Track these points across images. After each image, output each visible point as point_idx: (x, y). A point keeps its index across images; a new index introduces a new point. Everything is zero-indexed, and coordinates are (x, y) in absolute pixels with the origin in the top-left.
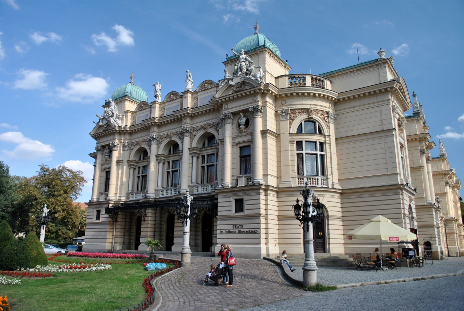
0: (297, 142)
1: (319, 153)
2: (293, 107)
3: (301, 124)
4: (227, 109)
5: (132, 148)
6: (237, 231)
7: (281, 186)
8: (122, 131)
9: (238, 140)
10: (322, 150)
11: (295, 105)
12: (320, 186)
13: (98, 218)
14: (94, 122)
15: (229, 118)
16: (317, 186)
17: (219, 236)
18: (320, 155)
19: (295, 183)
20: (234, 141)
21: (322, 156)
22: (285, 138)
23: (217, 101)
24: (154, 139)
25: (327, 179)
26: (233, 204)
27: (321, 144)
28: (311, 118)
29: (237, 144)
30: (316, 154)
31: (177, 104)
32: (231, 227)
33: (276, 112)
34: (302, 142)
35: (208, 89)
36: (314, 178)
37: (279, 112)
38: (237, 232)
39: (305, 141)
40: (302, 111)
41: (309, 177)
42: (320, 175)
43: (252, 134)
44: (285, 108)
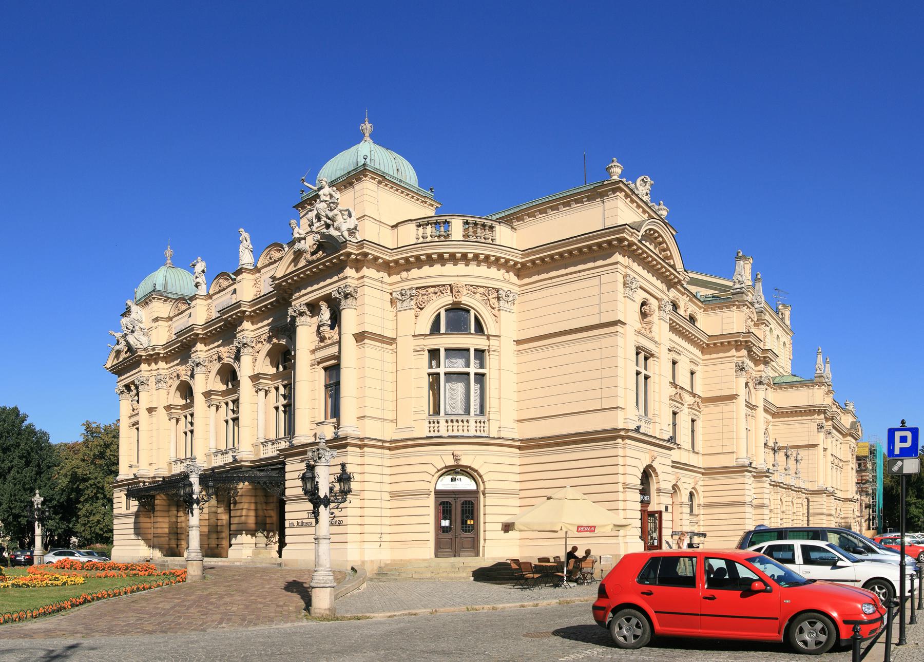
0: (429, 351)
1: (473, 370)
5: (169, 384)
11: (426, 278)
12: (472, 433)
13: (128, 508)
16: (466, 434)
18: (476, 374)
19: (422, 430)
20: (313, 357)
21: (480, 377)
22: (406, 345)
27: (480, 353)
28: (460, 303)
30: (468, 374)
34: (438, 350)
36: (460, 418)
37: (394, 294)
39: (446, 350)
40: (439, 289)
41: (449, 418)
44: (406, 285)
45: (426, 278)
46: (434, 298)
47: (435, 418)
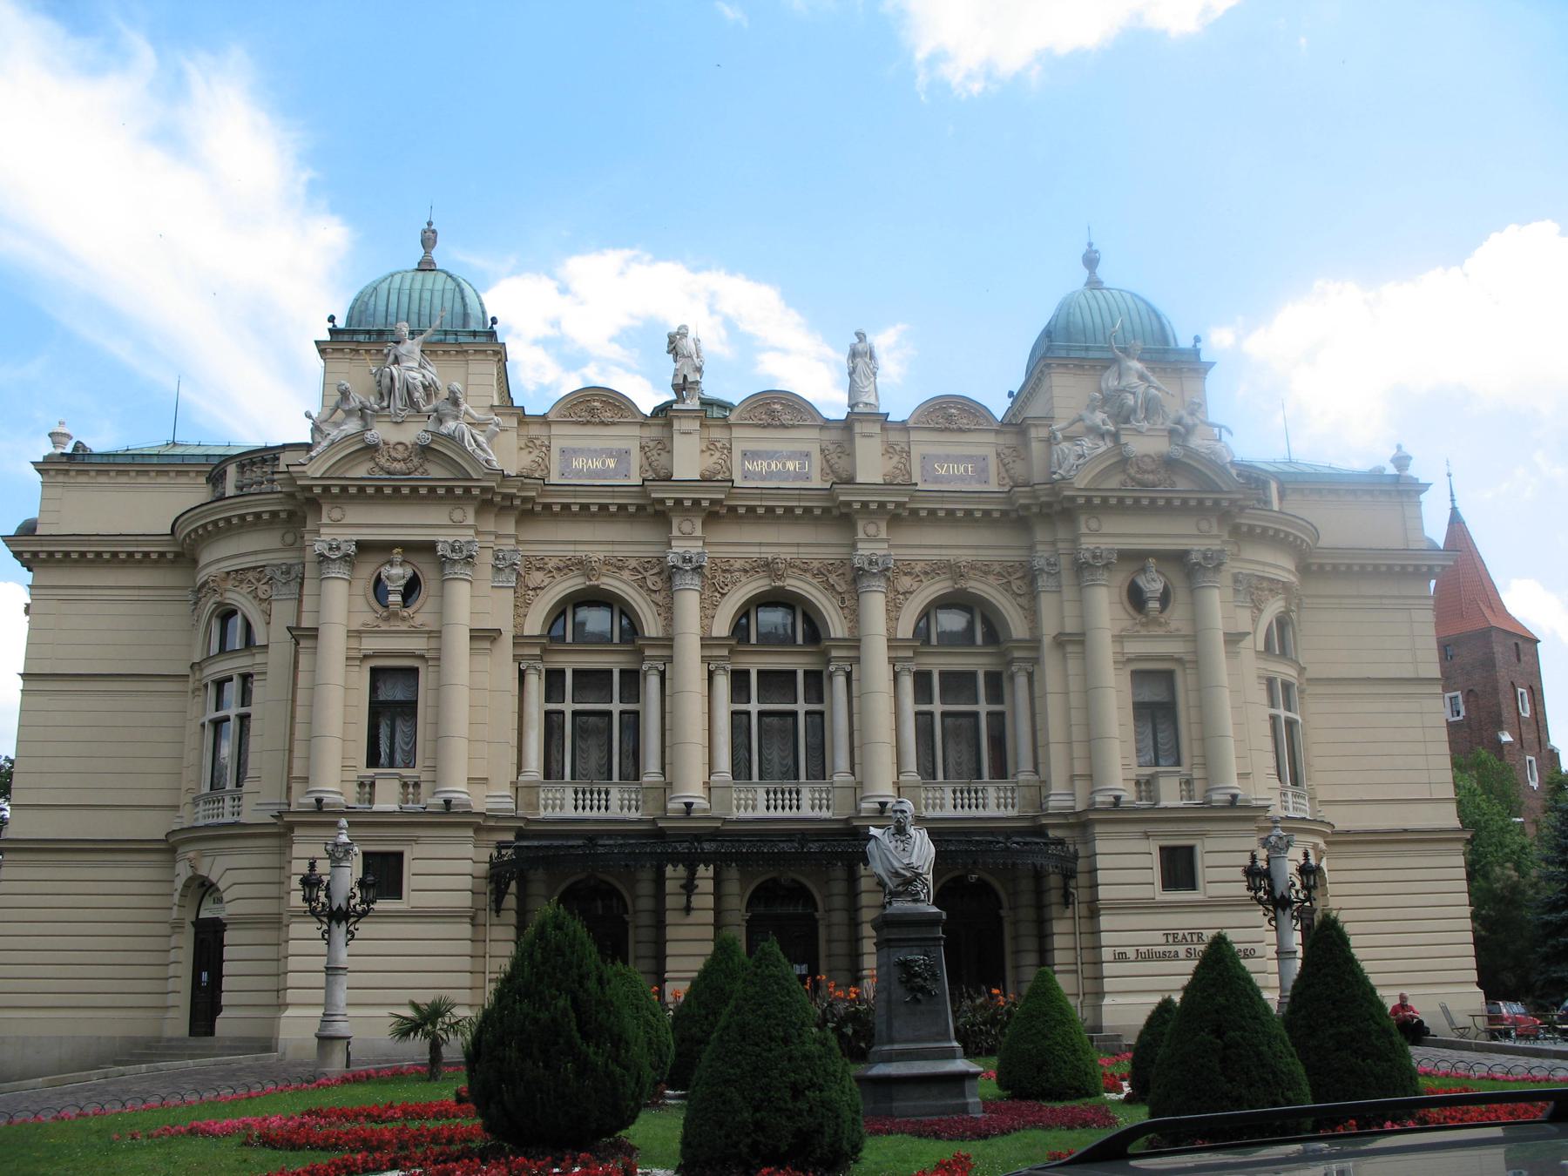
2: (1258, 570)
4: (1095, 533)
6: (1182, 950)
8: (505, 496)
9: (1134, 648)
14: (308, 415)
15: (1107, 566)
17: (1107, 969)
23: (1073, 499)
24: (698, 569)
26: (1155, 861)
29: (1129, 660)
31: (805, 447)
32: (1159, 937)
35: (960, 430)
38: (1182, 954)
40: (1277, 587)
43: (1195, 637)
45: (1264, 564)
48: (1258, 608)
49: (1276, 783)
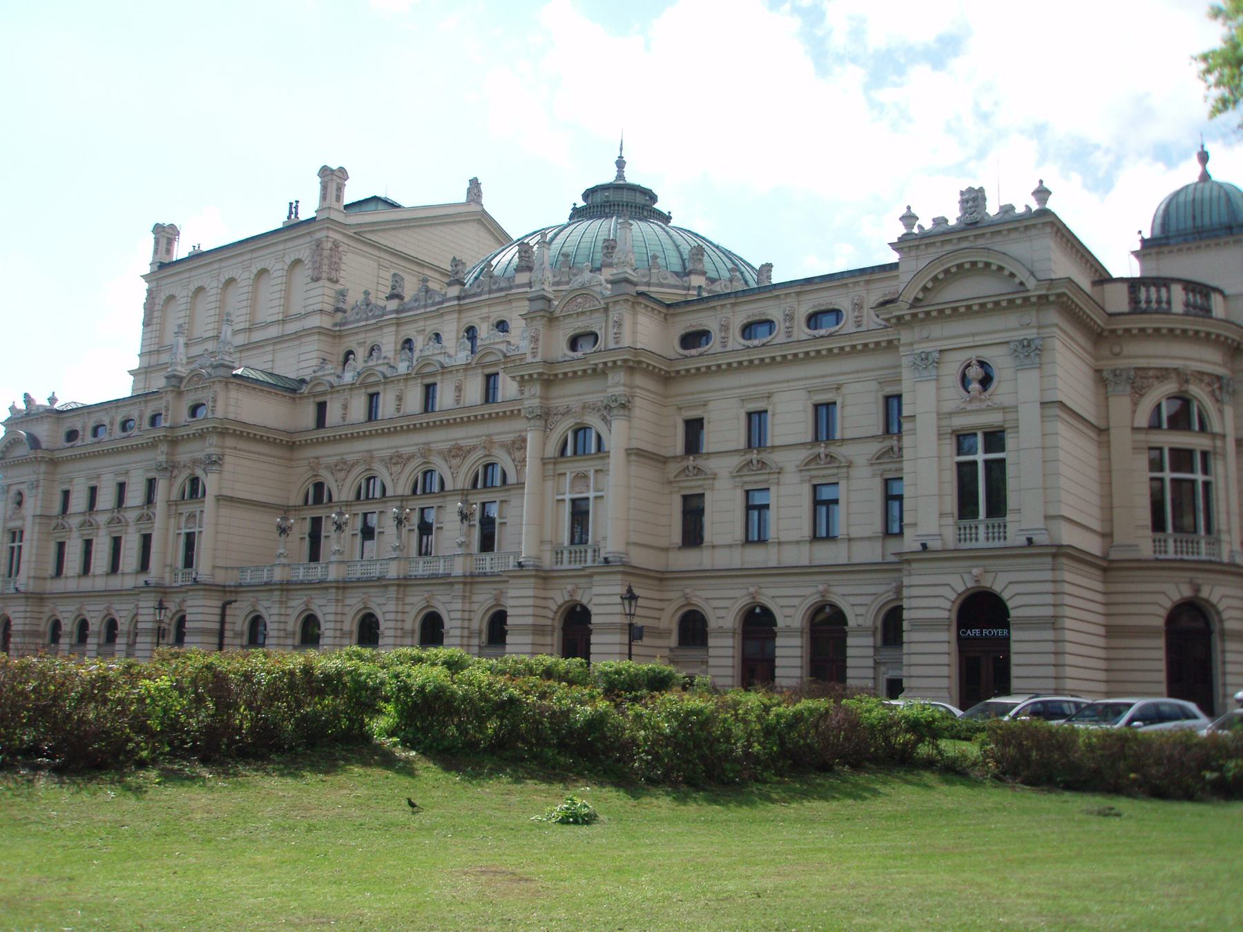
0: (1151, 448)
1: (1199, 477)
2: (1142, 363)
3: (1159, 406)
7: (1114, 555)
10: (1206, 471)
11: (1149, 357)
12: (1203, 557)
19: (1146, 549)
21: (1207, 485)
22: (1121, 438)
25: (1219, 541)
27: (1205, 455)
28: (1186, 392)
33: (1098, 371)
34: (1161, 449)
37: (1105, 374)
39: (1172, 450)
40: (1163, 374)
41: (1179, 536)
42: (1202, 532)
45: (1149, 357)
46: (1156, 383)
47: (1160, 535)
48: (1138, 392)
49: (1149, 532)
